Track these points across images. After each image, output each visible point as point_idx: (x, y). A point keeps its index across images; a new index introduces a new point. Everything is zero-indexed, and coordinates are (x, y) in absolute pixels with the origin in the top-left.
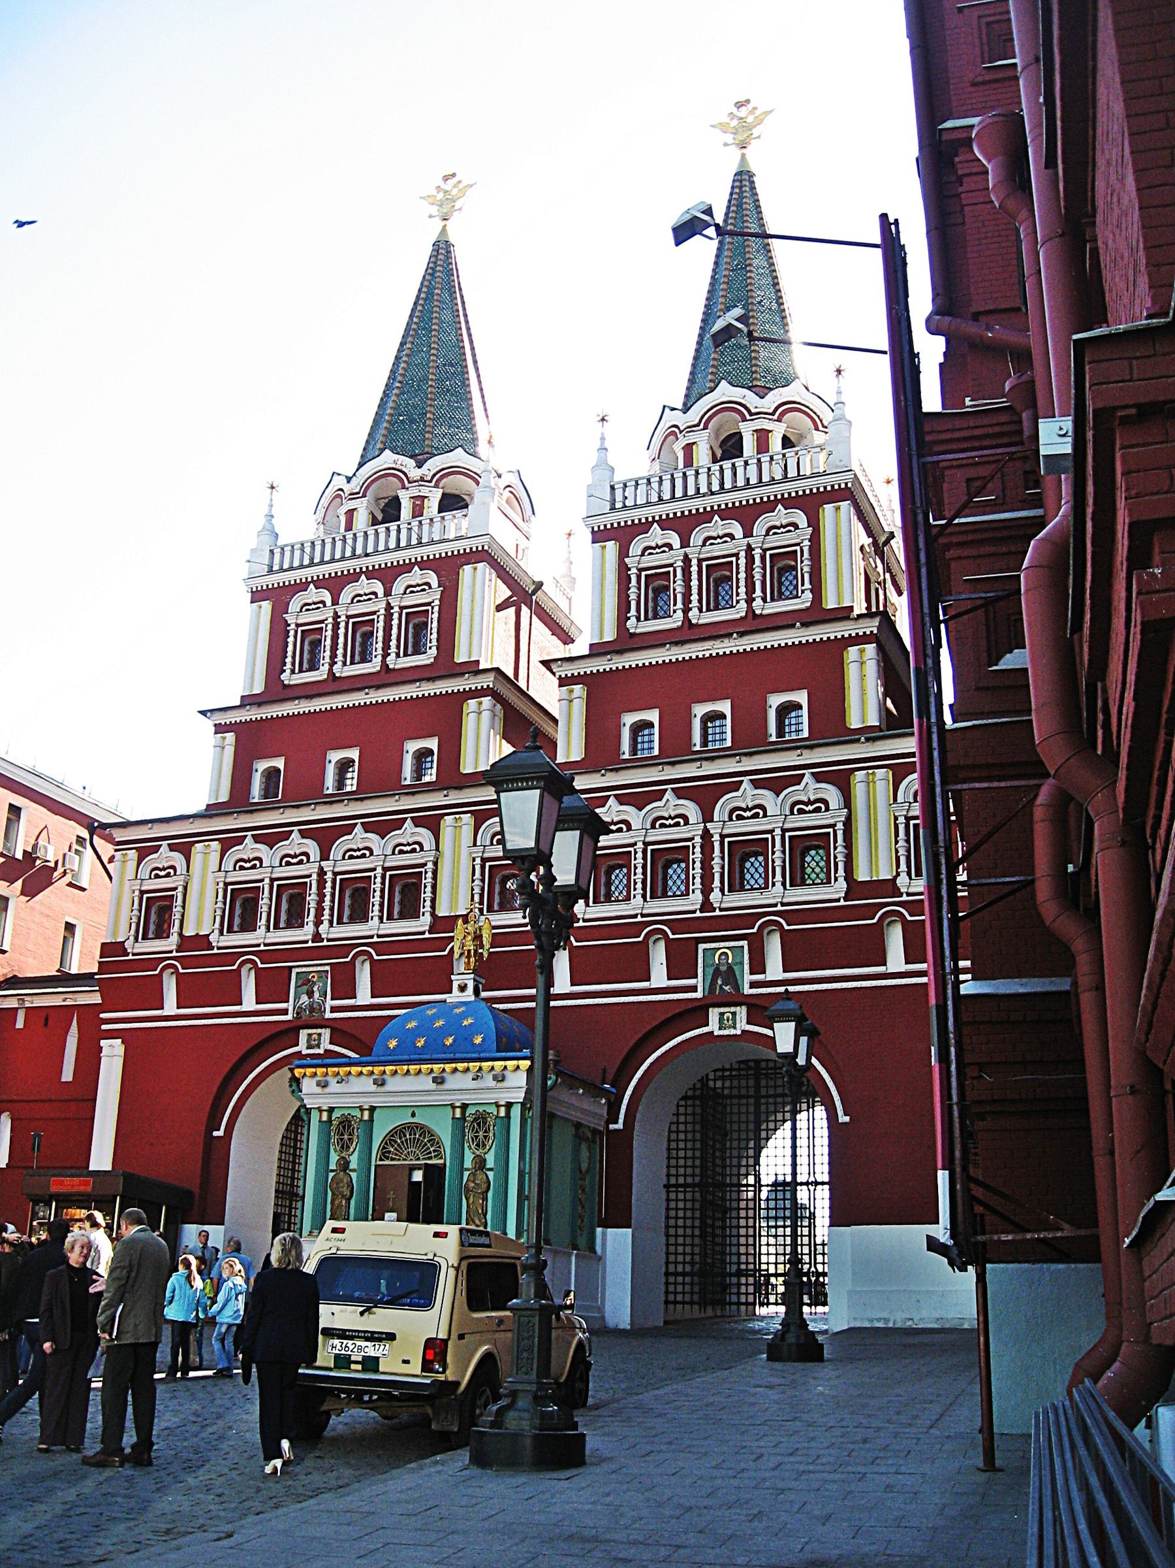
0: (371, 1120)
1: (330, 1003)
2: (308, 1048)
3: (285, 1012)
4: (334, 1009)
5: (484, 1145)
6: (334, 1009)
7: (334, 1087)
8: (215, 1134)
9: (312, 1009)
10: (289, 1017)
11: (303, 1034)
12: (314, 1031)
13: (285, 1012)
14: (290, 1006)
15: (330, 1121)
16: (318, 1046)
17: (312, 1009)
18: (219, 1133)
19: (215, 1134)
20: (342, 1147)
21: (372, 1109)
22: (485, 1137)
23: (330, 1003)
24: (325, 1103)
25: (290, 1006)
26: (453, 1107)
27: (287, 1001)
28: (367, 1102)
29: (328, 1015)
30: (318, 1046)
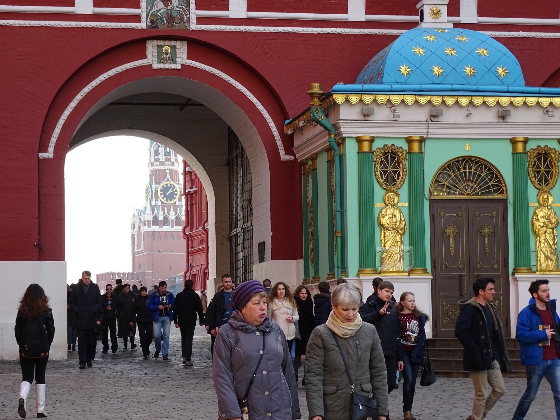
0: (421, 152)
1: (194, 13)
2: (161, 60)
3: (136, 18)
4: (200, 20)
5: (546, 180)
6: (200, 20)
7: (381, 114)
8: (42, 155)
9: (171, 18)
10: (143, 25)
11: (151, 48)
12: (167, 43)
13: (136, 18)
14: (142, 11)
15: (371, 152)
16: (175, 62)
17: (171, 18)
18: (49, 154)
19: (42, 155)
20: (387, 180)
21: (422, 141)
22: (548, 173)
23: (194, 13)
24: (366, 131)
25: (142, 11)
26: (514, 142)
27: (139, 7)
28: (416, 132)
29: (194, 26)
30: (173, 60)
